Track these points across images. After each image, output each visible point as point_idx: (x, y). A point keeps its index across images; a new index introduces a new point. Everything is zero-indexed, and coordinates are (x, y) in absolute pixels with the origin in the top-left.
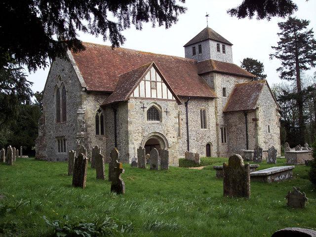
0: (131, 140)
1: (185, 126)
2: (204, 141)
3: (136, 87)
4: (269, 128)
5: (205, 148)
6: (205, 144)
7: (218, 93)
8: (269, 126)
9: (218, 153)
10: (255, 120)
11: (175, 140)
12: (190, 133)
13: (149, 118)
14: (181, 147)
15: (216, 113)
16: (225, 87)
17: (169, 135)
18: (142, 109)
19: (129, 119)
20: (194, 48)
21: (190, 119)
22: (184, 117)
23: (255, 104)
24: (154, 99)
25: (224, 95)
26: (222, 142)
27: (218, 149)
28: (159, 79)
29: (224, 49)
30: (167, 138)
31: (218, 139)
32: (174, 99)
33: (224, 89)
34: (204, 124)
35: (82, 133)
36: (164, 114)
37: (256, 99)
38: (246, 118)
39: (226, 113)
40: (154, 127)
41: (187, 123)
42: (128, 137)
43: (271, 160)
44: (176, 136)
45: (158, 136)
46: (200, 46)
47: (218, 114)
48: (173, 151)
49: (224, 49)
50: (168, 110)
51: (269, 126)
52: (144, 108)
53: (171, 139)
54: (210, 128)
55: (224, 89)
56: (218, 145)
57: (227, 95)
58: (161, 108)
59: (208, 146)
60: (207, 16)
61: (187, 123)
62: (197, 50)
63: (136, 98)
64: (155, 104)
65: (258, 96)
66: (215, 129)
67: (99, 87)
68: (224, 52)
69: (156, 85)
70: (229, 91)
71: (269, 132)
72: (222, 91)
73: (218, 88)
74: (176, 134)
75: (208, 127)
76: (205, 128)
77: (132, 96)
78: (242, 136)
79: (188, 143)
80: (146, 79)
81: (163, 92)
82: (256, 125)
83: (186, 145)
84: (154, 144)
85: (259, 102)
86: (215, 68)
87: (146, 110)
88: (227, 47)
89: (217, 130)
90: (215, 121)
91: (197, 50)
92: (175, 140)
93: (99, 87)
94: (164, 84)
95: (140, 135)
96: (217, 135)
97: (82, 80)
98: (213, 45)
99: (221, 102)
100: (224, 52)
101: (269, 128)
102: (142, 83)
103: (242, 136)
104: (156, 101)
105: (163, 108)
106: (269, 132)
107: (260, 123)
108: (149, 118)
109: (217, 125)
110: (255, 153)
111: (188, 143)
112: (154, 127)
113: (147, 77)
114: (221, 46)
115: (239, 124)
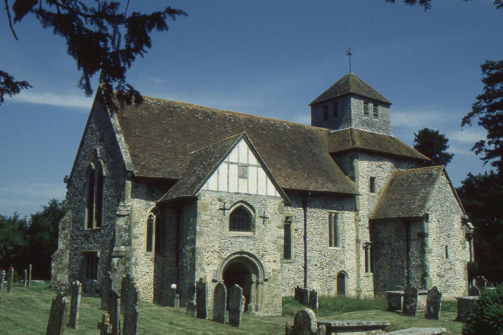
0: (200, 264)
1: (302, 241)
2: (334, 269)
4: (446, 250)
5: (335, 282)
6: (335, 274)
7: (362, 186)
8: (447, 246)
9: (359, 291)
10: (423, 236)
11: (277, 266)
12: (308, 254)
13: (233, 227)
14: (293, 278)
15: (357, 221)
16: (373, 176)
17: (267, 258)
18: (221, 212)
19: (198, 228)
20: (326, 108)
21: (310, 229)
22: (301, 225)
23: (422, 207)
25: (372, 189)
26: (367, 271)
27: (358, 282)
28: (253, 160)
29: (375, 110)
30: (262, 262)
31: (359, 266)
32: (278, 195)
33: (372, 180)
34: (334, 239)
35: (122, 247)
36: (258, 222)
37: (425, 199)
38: (408, 231)
39: (375, 224)
40: (241, 242)
41: (305, 238)
42: (193, 258)
43: (432, 310)
44: (278, 259)
45: (247, 259)
46: (335, 105)
47: (360, 223)
48: (272, 285)
49: (375, 110)
50: (267, 215)
51: (447, 246)
52: (224, 209)
53: (271, 262)
54: (346, 246)
55: (372, 180)
56: (358, 276)
57: (377, 189)
58: (254, 212)
59: (341, 277)
60: (349, 54)
61: (305, 238)
62: (331, 112)
64: (243, 205)
65: (428, 193)
66: (353, 247)
67: (156, 171)
68: (376, 116)
70: (382, 184)
72: (368, 183)
73: (361, 178)
74: (279, 255)
75: (341, 244)
76: (336, 245)
78: (399, 263)
79: (306, 271)
80: (231, 161)
82: (424, 244)
83: (302, 274)
84: (240, 272)
85: (430, 203)
86: (358, 144)
87: (228, 213)
88: (380, 109)
89: (358, 251)
90: (354, 235)
91: (331, 112)
92: (277, 266)
93: (156, 171)
94: (261, 170)
95: (216, 255)
96: (358, 259)
97: (127, 158)
98: (356, 105)
99: (367, 204)
100: (376, 116)
101: (446, 250)
102: (223, 167)
103: (399, 263)
105: (257, 211)
107: (431, 241)
108: (233, 227)
109: (358, 241)
110: (405, 296)
111: (306, 271)
112: (241, 242)
113: (233, 157)
114: (371, 105)
115: (396, 241)
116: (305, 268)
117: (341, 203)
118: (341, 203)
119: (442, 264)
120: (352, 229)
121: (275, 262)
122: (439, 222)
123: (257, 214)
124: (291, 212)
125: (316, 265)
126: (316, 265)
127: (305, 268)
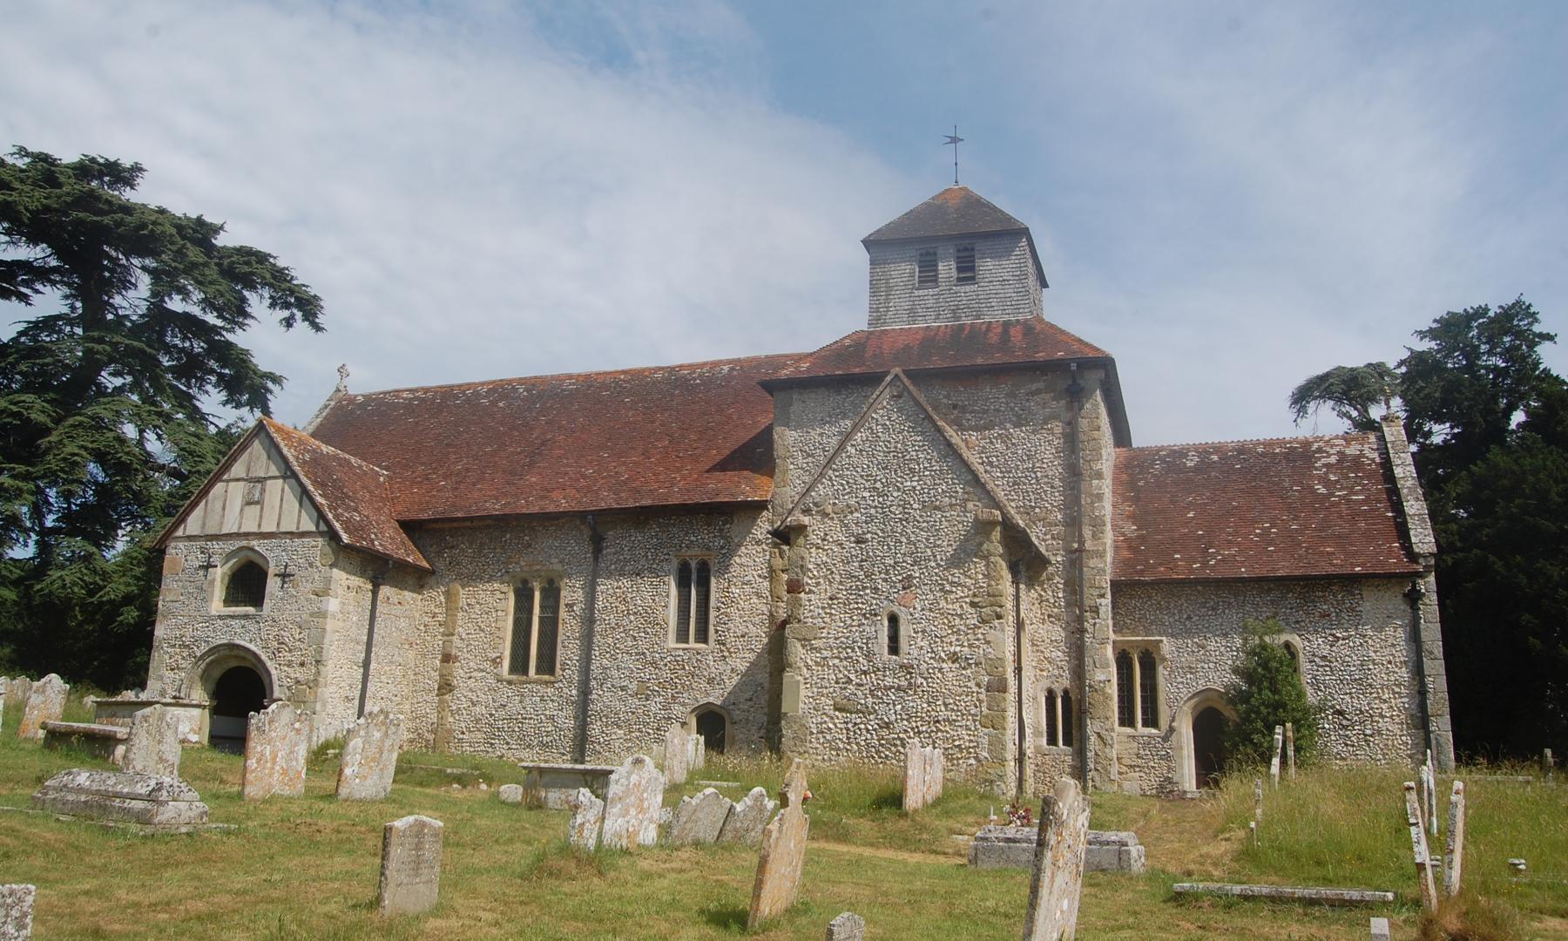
3: (194, 505)
14: (552, 718)
18: (201, 573)
24: (247, 535)
32: (323, 527)
34: (697, 621)
36: (273, 584)
51: (894, 620)
52: (207, 567)
63: (190, 538)
69: (263, 490)
71: (894, 649)
77: (180, 533)
81: (282, 508)
102: (219, 488)
104: (254, 543)
105: (272, 564)
106: (894, 649)
113: (238, 469)
116: (585, 692)
117: (721, 530)
118: (721, 530)
119: (865, 673)
120: (759, 595)
121: (302, 664)
122: (860, 541)
123: (272, 571)
124: (559, 567)
125: (623, 689)
126: (623, 689)
127: (585, 692)
